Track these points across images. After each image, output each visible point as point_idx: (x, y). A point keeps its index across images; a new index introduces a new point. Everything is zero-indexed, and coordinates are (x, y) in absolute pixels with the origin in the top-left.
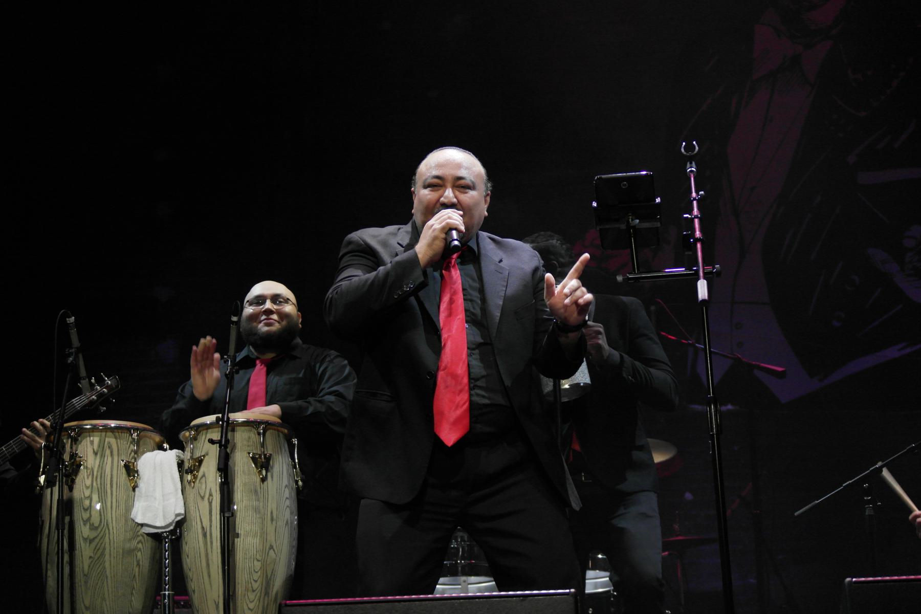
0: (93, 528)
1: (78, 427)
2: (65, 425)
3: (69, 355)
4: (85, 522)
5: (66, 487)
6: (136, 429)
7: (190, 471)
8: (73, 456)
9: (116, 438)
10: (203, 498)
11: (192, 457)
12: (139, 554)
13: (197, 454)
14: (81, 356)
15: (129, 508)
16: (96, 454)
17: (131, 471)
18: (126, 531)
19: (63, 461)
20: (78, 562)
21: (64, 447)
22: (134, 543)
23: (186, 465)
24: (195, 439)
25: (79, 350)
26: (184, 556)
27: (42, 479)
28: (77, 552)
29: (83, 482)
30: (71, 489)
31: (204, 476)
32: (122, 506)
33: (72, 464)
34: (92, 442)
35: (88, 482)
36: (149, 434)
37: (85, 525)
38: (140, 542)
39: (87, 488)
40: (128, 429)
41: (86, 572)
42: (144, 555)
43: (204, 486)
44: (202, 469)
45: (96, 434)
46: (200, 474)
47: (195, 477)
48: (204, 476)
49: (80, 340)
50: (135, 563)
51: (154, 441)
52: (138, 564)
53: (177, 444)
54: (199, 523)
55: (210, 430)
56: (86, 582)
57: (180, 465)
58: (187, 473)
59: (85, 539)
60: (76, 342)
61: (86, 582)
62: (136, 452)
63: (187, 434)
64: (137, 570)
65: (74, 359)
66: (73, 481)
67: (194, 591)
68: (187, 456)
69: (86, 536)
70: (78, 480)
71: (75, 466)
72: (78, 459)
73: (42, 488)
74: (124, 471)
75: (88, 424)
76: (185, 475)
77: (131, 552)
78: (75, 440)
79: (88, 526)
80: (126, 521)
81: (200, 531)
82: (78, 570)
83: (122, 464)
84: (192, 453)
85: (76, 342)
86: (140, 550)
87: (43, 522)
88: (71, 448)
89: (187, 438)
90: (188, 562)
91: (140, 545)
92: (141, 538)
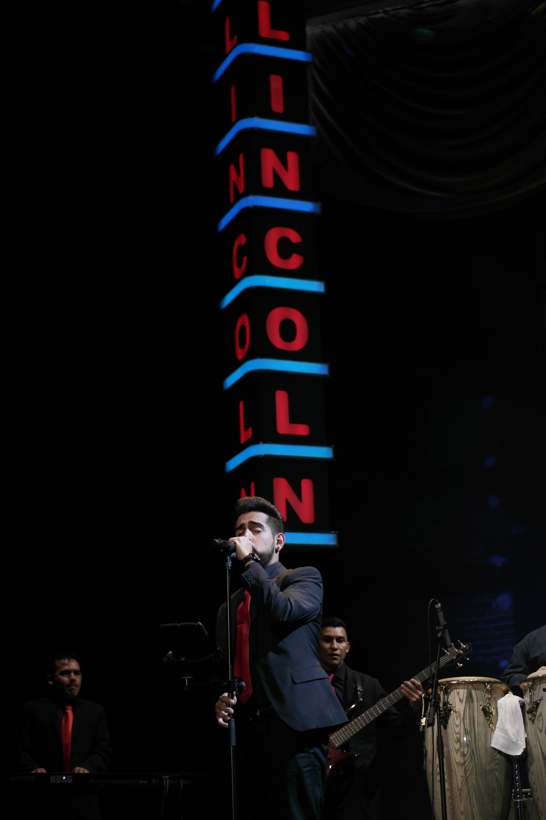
0: (464, 755)
1: (447, 682)
2: (440, 681)
3: (439, 631)
4: (457, 751)
5: (442, 726)
6: (489, 682)
7: (530, 712)
8: (445, 704)
9: (475, 689)
10: (541, 731)
11: (531, 701)
12: (497, 773)
13: (535, 699)
14: (447, 631)
15: (488, 739)
16: (461, 701)
17: (487, 713)
18: (486, 757)
19: (440, 708)
20: (454, 780)
21: (439, 699)
22: (493, 765)
23: (527, 708)
24: (532, 688)
25: (445, 627)
26: (530, 774)
27: (423, 721)
28: (454, 774)
29: (454, 721)
30: (445, 728)
31: (541, 715)
32: (483, 738)
33: (445, 710)
34: (458, 693)
35: (457, 722)
36: (498, 685)
37: (457, 753)
38: (497, 764)
39: (457, 726)
40: (484, 683)
41: (460, 787)
42: (500, 774)
43: (541, 723)
44: (539, 710)
45: (460, 687)
46: (538, 714)
47: (535, 716)
48: (541, 715)
49: (446, 619)
50: (494, 780)
51: (502, 689)
52: (497, 780)
53: (519, 692)
54: (539, 750)
55: (543, 681)
56: (460, 795)
57: (523, 706)
58: (528, 712)
59: (458, 764)
60: (443, 622)
61: (460, 795)
62: (489, 699)
63: (526, 684)
64: (495, 784)
65: (443, 634)
66: (447, 722)
67: (538, 799)
68: (527, 699)
69: (458, 761)
70: (450, 721)
71: (448, 711)
72: (449, 706)
73: (424, 726)
74: (482, 713)
75: (454, 680)
76: (527, 715)
77: (491, 771)
78: (446, 693)
79: (459, 754)
80: (486, 749)
81: (540, 755)
82: (455, 786)
83: (481, 708)
84: (531, 698)
85: (443, 622)
86: (497, 770)
87: (426, 751)
88: (444, 698)
89: (525, 687)
90: (532, 778)
91: (497, 767)
92: (497, 761)
